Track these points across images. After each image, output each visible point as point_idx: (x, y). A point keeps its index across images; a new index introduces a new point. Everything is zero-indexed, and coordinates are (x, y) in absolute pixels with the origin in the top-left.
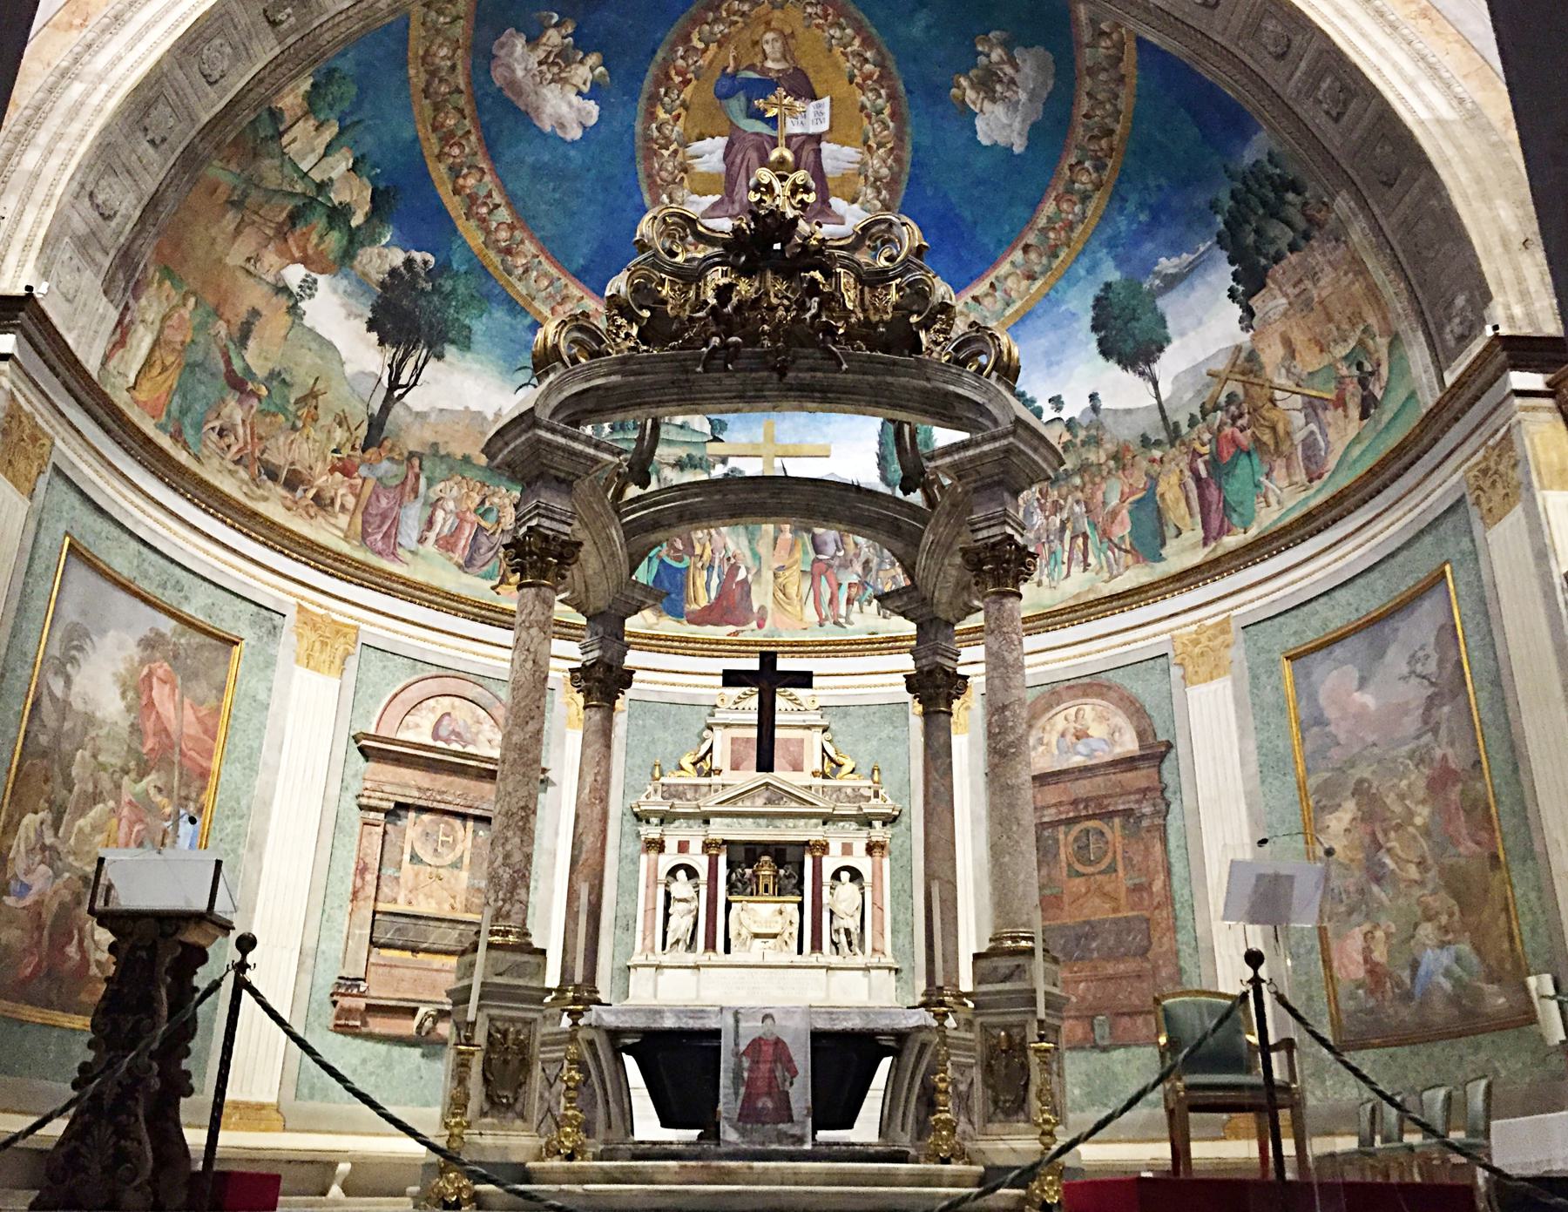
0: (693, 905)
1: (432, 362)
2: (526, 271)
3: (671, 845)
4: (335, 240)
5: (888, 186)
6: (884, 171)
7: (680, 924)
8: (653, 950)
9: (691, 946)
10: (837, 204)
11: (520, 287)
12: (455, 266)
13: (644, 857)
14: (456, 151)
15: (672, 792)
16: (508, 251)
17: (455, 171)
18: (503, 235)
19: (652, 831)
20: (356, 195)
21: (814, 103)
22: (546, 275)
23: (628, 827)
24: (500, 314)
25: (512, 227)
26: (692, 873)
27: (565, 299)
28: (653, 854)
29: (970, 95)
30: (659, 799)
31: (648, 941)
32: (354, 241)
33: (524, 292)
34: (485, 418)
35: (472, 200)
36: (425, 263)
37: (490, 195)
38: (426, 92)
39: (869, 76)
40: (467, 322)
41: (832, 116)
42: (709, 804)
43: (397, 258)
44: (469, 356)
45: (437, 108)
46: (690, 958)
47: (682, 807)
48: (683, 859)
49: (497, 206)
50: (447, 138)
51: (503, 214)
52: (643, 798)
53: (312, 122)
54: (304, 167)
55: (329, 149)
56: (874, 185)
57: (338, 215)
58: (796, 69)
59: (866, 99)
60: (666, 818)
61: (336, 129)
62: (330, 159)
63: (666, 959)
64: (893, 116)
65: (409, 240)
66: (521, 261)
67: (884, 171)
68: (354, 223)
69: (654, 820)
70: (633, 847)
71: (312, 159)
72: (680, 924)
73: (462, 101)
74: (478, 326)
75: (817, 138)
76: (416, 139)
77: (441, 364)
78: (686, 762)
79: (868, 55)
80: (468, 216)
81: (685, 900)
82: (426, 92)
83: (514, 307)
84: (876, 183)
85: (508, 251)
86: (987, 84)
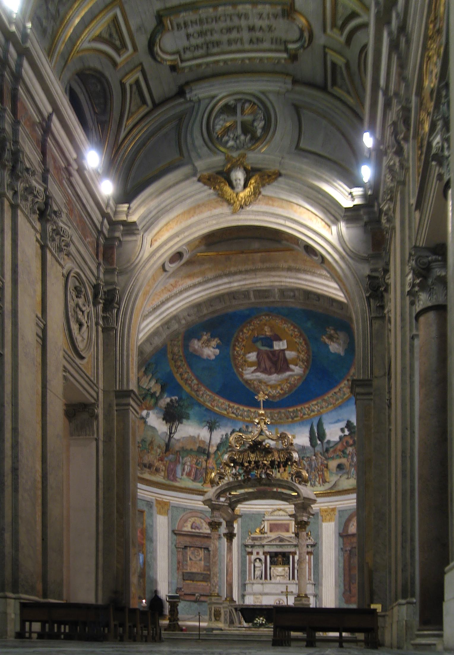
0: (261, 568)
1: (180, 425)
2: (203, 394)
3: (255, 553)
4: (153, 401)
5: (307, 362)
6: (305, 358)
7: (258, 573)
8: (251, 580)
9: (261, 578)
10: (292, 366)
11: (202, 400)
12: (183, 398)
13: (248, 557)
14: (181, 370)
15: (254, 539)
16: (197, 391)
17: (181, 375)
18: (196, 387)
19: (249, 550)
20: (156, 388)
21: (281, 343)
22: (208, 395)
23: (243, 548)
24: (197, 408)
25: (198, 384)
26: (260, 560)
27: (214, 400)
28: (250, 556)
29: (327, 341)
30: (251, 541)
31: (250, 578)
32: (157, 399)
33: (203, 401)
34: (195, 438)
35: (186, 380)
36: (176, 399)
37: (191, 378)
38: (172, 359)
39: (297, 335)
40: (188, 412)
41: (287, 344)
42: (264, 542)
43: (168, 400)
44: (189, 421)
45: (175, 362)
46: (261, 581)
47: (257, 543)
48: (258, 557)
49: (193, 380)
50: (179, 367)
51: (195, 381)
52: (247, 541)
53: (145, 377)
54: (144, 387)
55: (150, 381)
56: (302, 361)
57: (153, 395)
58: (275, 334)
59: (297, 340)
60: (253, 546)
61: (151, 375)
62: (151, 383)
63: (255, 582)
64: (306, 344)
65: (171, 394)
66: (201, 393)
67: (305, 358)
68: (157, 396)
69: (250, 547)
70: (244, 554)
71: (146, 384)
72: (258, 573)
73: (182, 358)
74: (191, 412)
75: (283, 350)
76: (171, 370)
77: (182, 425)
78: (258, 531)
79: (296, 330)
80: (186, 384)
81: (259, 567)
82: (172, 359)
83: (200, 405)
84: (303, 361)
85: (197, 391)
86: (331, 338)
